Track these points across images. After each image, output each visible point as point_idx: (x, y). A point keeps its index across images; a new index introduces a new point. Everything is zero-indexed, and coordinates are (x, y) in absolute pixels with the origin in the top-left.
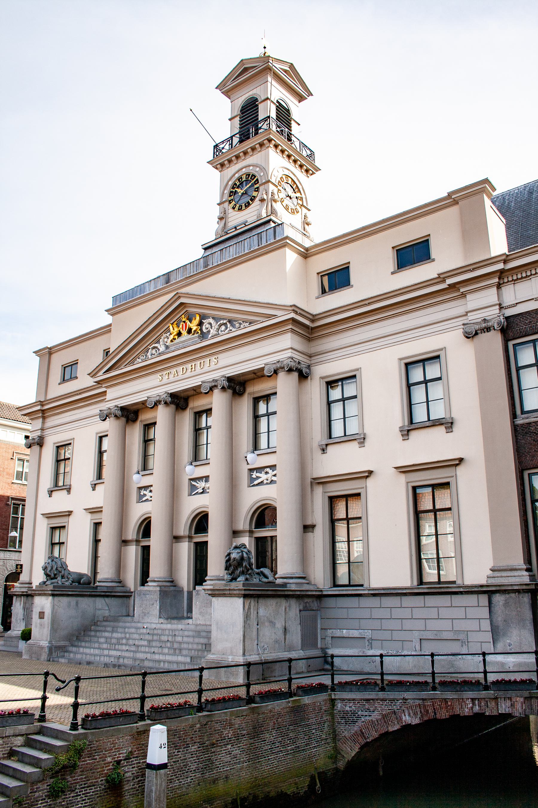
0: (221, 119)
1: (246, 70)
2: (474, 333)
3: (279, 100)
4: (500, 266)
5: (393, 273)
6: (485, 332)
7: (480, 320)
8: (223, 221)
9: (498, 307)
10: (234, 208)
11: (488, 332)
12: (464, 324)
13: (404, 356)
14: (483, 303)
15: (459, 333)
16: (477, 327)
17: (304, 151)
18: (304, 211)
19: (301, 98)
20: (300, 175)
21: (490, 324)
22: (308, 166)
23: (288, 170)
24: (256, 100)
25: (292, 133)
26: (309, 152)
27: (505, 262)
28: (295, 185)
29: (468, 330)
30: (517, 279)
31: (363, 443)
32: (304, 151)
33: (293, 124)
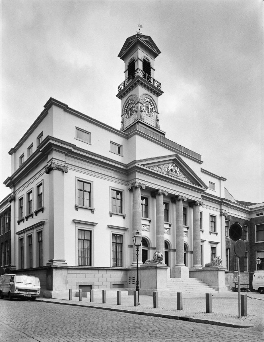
0: (118, 74)
1: (130, 43)
3: (144, 59)
8: (123, 124)
10: (126, 117)
17: (156, 84)
18: (156, 114)
19: (155, 55)
20: (154, 96)
22: (158, 92)
23: (149, 95)
24: (134, 60)
25: (151, 76)
26: (158, 84)
28: (151, 102)
32: (156, 84)
33: (152, 70)
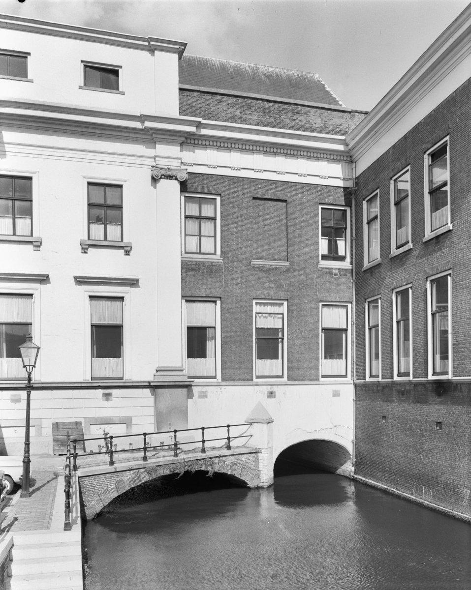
2: (159, 177)
4: (192, 129)
5: (80, 88)
6: (167, 179)
7: (166, 167)
9: (180, 161)
11: (170, 179)
12: (153, 167)
13: (89, 175)
14: (169, 154)
15: (147, 174)
16: (163, 172)
21: (174, 173)
27: (197, 127)
29: (155, 173)
30: (198, 144)
31: (39, 246)
